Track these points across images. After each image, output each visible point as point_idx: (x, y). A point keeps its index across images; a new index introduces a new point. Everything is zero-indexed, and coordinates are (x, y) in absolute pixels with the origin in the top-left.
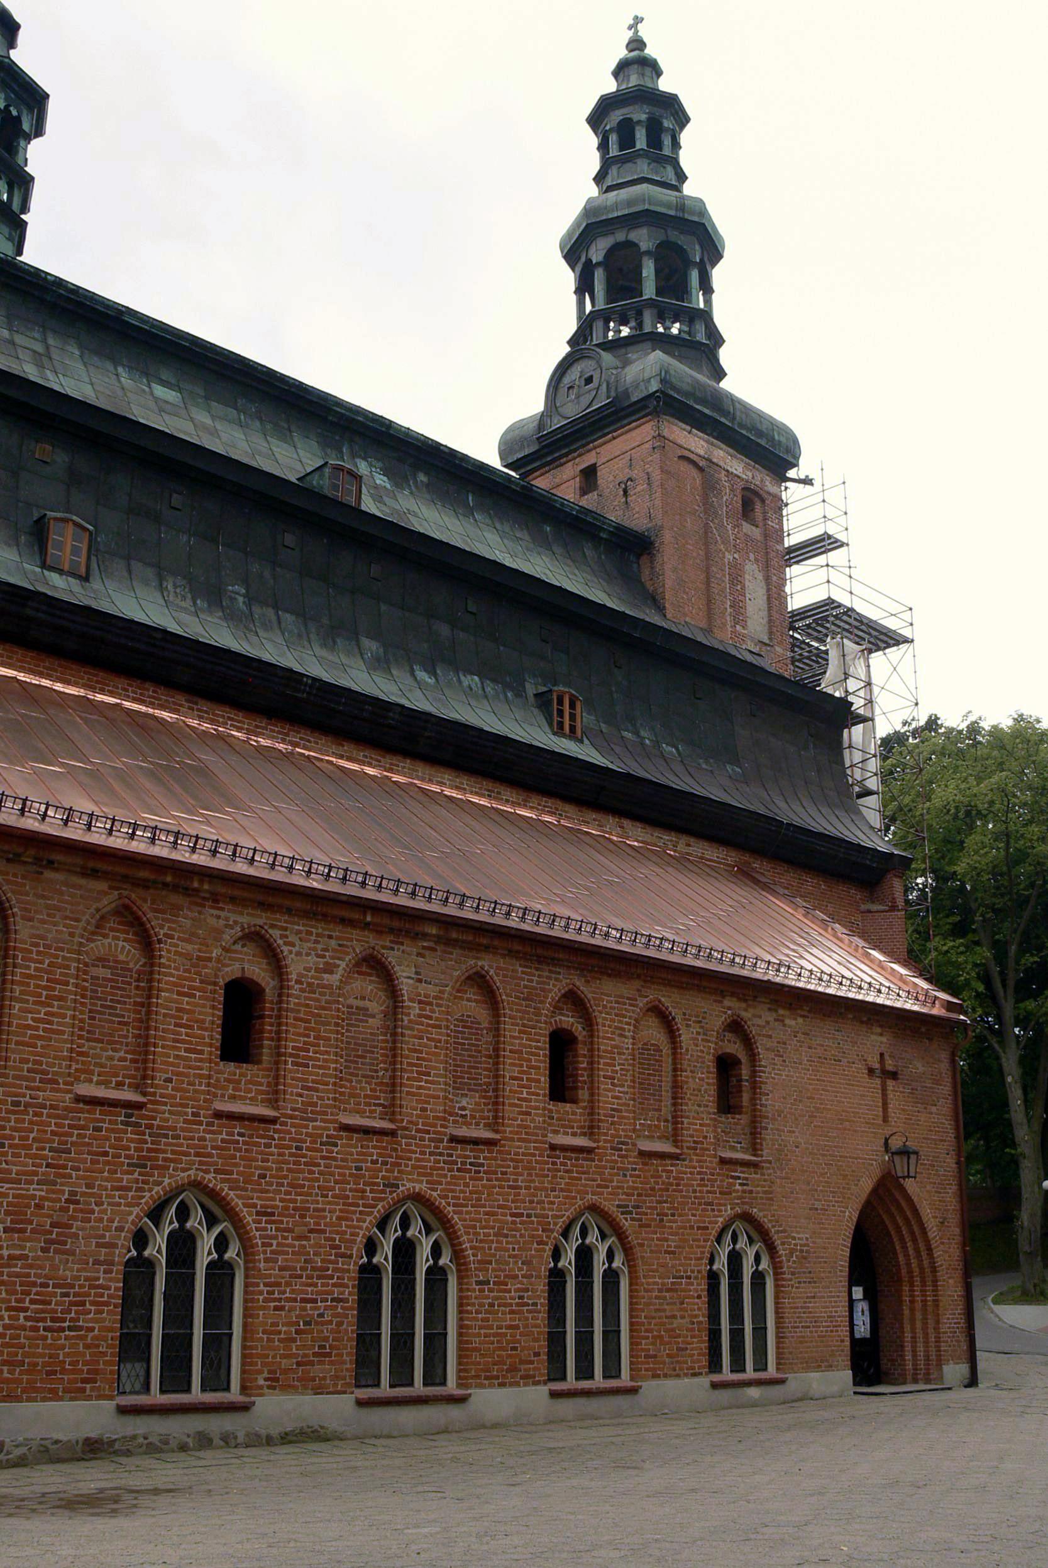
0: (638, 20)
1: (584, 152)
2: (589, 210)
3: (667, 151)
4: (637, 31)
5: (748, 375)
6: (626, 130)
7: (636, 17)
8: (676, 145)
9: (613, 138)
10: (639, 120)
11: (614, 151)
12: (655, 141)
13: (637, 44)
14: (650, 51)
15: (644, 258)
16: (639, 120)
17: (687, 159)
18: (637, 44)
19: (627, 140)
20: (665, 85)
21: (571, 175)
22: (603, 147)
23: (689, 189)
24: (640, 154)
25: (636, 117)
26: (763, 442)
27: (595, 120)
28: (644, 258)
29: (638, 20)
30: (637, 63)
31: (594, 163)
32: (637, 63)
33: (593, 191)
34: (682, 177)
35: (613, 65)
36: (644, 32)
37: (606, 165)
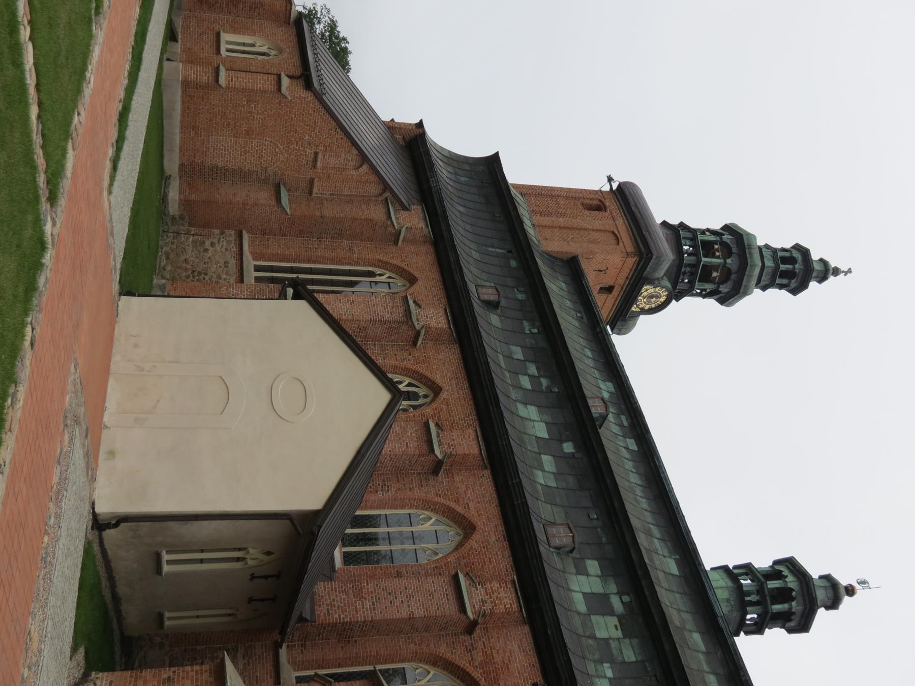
1: (782, 241)
2: (752, 237)
3: (778, 281)
6: (791, 260)
8: (781, 287)
9: (787, 254)
10: (796, 270)
11: (780, 254)
12: (784, 274)
13: (836, 272)
14: (831, 279)
16: (796, 270)
17: (773, 292)
18: (836, 272)
19: (785, 260)
20: (813, 284)
22: (783, 250)
23: (757, 292)
24: (777, 267)
25: (797, 266)
27: (797, 247)
30: (826, 272)
31: (776, 245)
32: (826, 272)
33: (760, 242)
34: (764, 289)
37: (775, 251)
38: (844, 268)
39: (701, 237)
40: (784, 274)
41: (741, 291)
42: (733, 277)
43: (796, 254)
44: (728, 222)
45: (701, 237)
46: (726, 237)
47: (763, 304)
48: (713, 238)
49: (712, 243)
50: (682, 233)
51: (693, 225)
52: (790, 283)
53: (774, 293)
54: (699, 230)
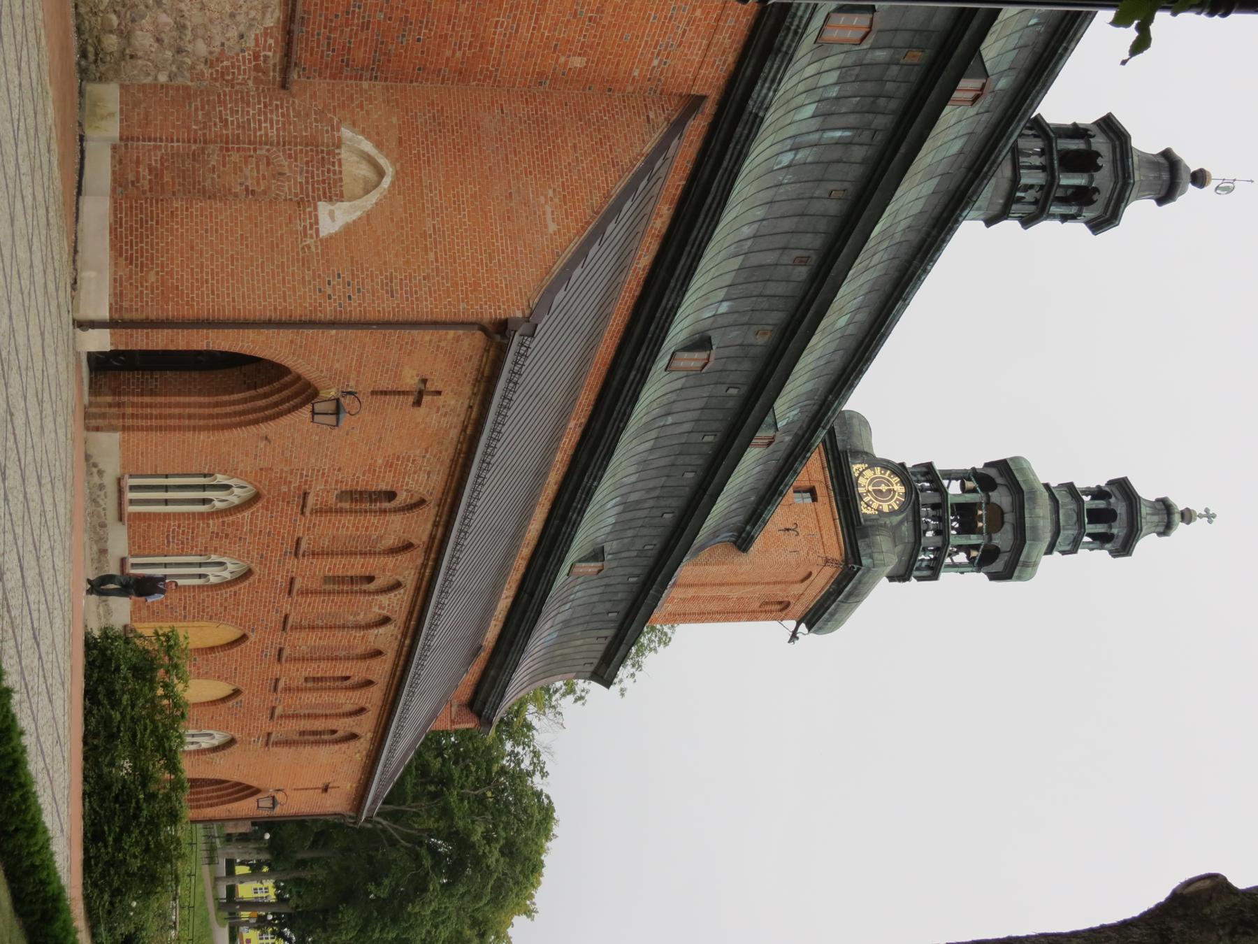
0: (1210, 517)
4: (1201, 516)
5: (886, 602)
7: (1214, 516)
10: (1113, 517)
13: (1187, 516)
14: (1181, 528)
15: (989, 520)
16: (1113, 517)
18: (1187, 516)
26: (826, 615)
28: (989, 520)
29: (1210, 517)
30: (1167, 516)
32: (1167, 516)
36: (1200, 523)
38: (1199, 510)
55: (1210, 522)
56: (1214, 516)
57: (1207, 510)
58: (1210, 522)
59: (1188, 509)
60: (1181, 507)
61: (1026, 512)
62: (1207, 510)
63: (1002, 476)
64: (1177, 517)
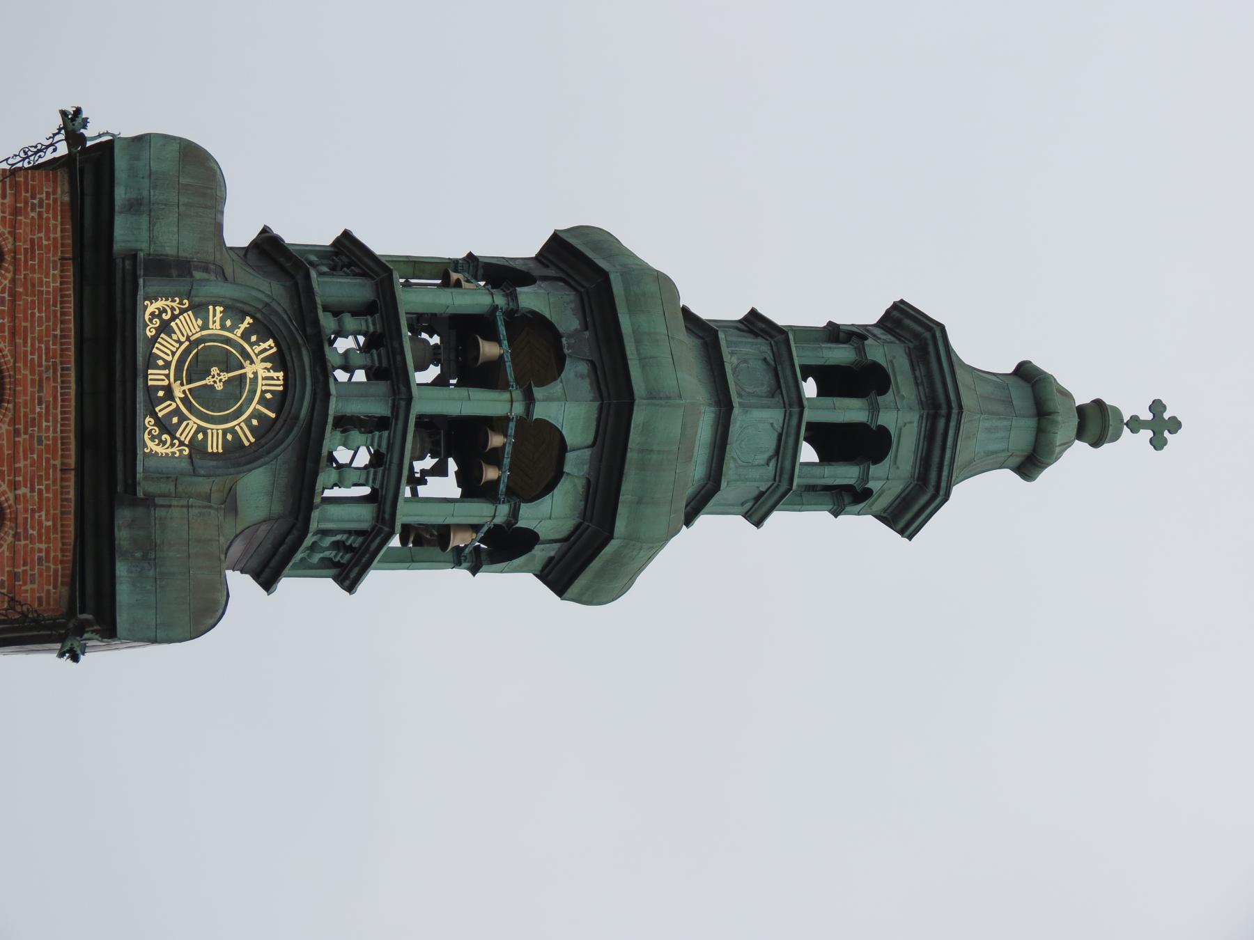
4: (1135, 424)
7: (1175, 425)
8: (843, 499)
9: (841, 355)
10: (886, 417)
13: (1097, 423)
14: (1077, 458)
16: (886, 417)
18: (1097, 423)
21: (751, 248)
22: (834, 333)
29: (1161, 425)
30: (1043, 420)
32: (1043, 420)
35: (1043, 363)
38: (1133, 405)
39: (418, 297)
40: (835, 443)
41: (621, 526)
42: (577, 465)
43: (888, 354)
44: (564, 223)
45: (418, 297)
46: (530, 298)
47: (744, 582)
48: (475, 298)
49: (480, 325)
50: (332, 288)
51: (383, 242)
52: (865, 477)
53: (801, 529)
54: (418, 266)
55: (1158, 443)
56: (1175, 425)
57: (1157, 407)
58: (1158, 443)
59: (1098, 403)
60: (1082, 398)
61: (622, 511)
62: (1157, 407)
63: (580, 293)
64: (1066, 425)
